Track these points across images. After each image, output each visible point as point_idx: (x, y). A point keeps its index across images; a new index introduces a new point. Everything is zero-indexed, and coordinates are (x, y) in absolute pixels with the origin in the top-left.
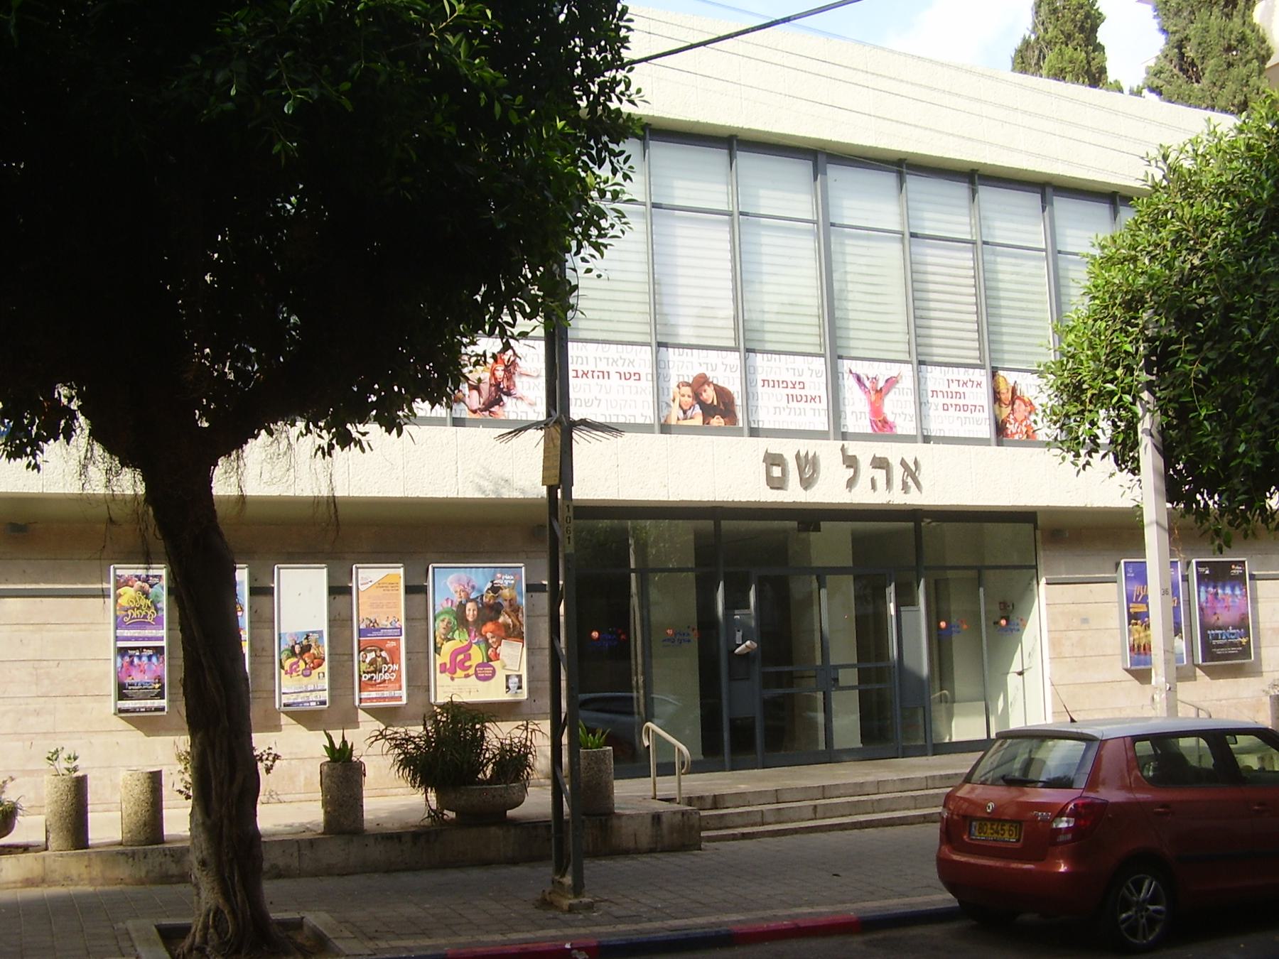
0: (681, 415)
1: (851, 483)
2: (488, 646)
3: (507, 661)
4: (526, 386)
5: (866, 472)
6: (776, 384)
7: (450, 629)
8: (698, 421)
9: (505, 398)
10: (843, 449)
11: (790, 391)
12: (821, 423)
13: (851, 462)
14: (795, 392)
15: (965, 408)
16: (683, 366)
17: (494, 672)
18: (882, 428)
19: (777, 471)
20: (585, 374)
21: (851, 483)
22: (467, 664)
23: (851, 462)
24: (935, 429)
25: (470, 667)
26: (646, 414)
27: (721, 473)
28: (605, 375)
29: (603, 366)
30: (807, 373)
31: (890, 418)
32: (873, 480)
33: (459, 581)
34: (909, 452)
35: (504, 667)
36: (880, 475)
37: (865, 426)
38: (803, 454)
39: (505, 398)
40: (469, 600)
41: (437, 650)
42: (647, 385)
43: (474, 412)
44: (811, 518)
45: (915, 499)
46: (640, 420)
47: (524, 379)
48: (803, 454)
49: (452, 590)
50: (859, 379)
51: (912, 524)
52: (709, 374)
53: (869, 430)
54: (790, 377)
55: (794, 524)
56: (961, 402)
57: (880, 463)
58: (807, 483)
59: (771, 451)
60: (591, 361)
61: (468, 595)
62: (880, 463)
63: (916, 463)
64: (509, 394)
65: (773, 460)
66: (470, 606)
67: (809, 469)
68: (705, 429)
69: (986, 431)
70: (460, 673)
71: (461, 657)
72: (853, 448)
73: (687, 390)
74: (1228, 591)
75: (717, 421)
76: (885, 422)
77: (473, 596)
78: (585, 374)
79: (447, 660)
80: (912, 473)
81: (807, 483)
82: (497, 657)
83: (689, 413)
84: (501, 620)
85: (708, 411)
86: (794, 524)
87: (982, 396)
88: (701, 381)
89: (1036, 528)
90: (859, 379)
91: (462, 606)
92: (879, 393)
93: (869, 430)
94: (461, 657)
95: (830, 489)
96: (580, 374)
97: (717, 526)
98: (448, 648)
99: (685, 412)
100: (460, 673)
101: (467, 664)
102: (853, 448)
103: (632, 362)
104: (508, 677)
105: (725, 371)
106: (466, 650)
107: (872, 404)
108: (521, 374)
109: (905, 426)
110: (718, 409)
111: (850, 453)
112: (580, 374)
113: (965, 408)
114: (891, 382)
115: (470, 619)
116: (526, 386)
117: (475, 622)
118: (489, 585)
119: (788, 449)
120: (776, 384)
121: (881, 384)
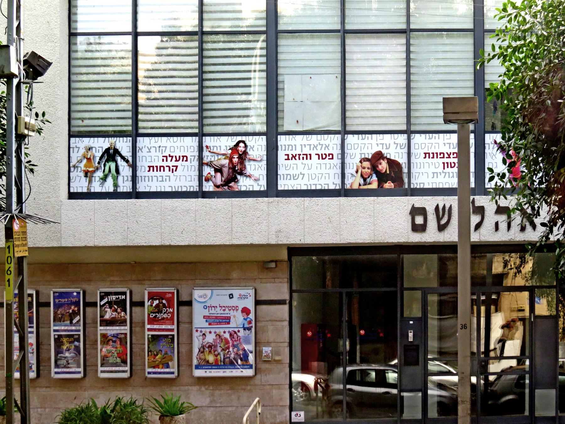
0: (362, 181)
4: (253, 167)
8: (375, 186)
9: (239, 177)
16: (361, 148)
28: (308, 156)
38: (441, 207)
39: (239, 177)
42: (337, 161)
47: (252, 163)
48: (441, 207)
52: (384, 151)
58: (441, 228)
59: (417, 205)
60: (299, 148)
64: (241, 174)
73: (367, 164)
75: (389, 185)
78: (294, 157)
83: (368, 180)
85: (382, 178)
88: (379, 156)
96: (290, 157)
99: (365, 180)
105: (393, 147)
108: (250, 160)
111: (477, 204)
112: (290, 157)
116: (253, 167)
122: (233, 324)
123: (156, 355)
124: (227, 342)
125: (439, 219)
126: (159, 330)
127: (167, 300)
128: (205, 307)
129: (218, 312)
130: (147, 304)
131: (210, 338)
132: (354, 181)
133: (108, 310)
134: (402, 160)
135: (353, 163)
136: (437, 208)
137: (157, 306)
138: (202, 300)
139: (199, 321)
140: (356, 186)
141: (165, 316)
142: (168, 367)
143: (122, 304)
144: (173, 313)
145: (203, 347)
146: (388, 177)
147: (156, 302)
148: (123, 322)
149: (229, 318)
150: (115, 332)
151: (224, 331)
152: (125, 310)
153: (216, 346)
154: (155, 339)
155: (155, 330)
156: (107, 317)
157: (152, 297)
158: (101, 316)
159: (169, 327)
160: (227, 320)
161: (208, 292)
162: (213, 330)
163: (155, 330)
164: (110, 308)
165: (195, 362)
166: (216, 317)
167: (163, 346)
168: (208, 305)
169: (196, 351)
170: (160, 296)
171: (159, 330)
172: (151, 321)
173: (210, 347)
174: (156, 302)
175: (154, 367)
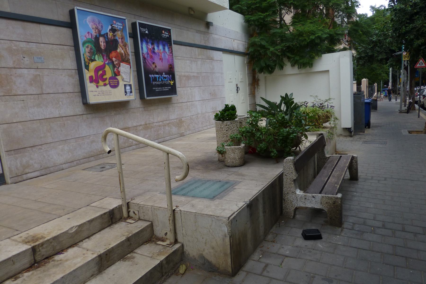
2: (114, 66)
3: (124, 77)
7: (92, 53)
17: (118, 82)
22: (105, 77)
25: (106, 79)
33: (93, 21)
35: (123, 80)
40: (101, 35)
41: (87, 67)
49: (90, 26)
61: (99, 32)
66: (101, 39)
70: (101, 83)
71: (100, 72)
77: (102, 33)
79: (92, 74)
82: (119, 72)
84: (118, 51)
91: (97, 39)
94: (100, 72)
98: (93, 65)
100: (101, 83)
101: (105, 77)
104: (125, 85)
106: (102, 68)
115: (103, 48)
117: (106, 49)
118: (110, 27)
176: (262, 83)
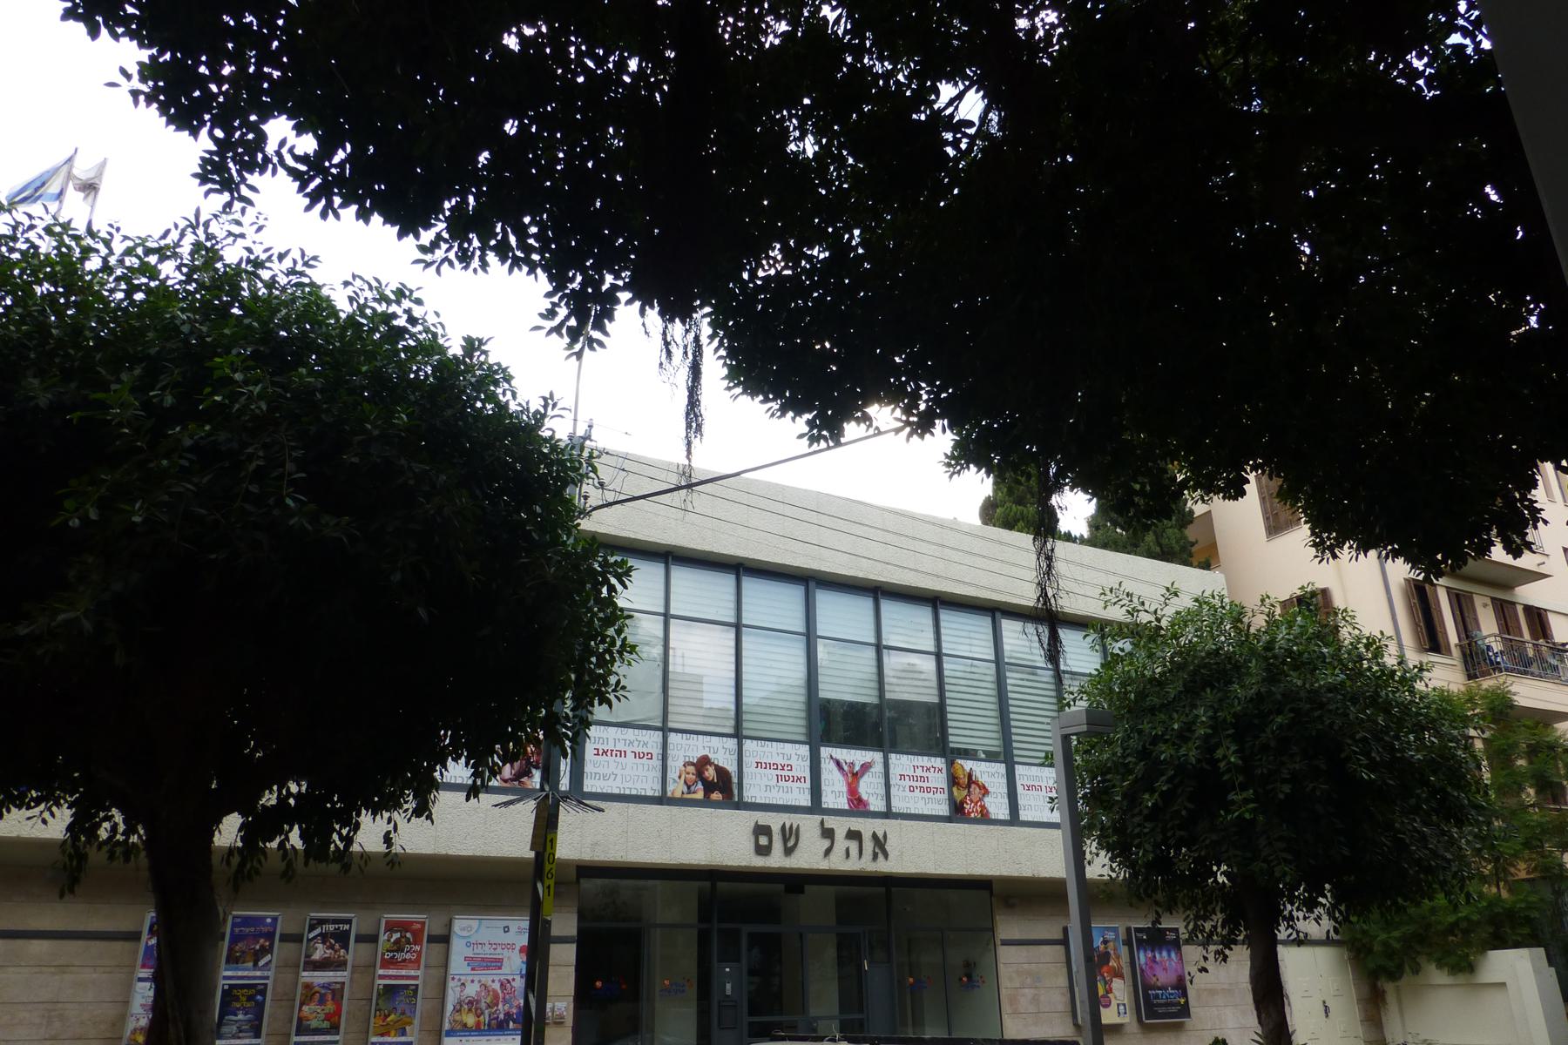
1: (828, 852)
5: (841, 842)
6: (767, 766)
8: (700, 795)
10: (822, 823)
11: (779, 772)
12: (805, 800)
13: (828, 834)
14: (783, 772)
15: (928, 790)
16: (685, 750)
18: (858, 806)
19: (763, 841)
20: (605, 752)
21: (828, 852)
23: (828, 834)
24: (898, 805)
26: (651, 787)
27: (719, 840)
29: (620, 746)
30: (794, 758)
31: (865, 797)
32: (847, 851)
34: (879, 826)
36: (854, 846)
37: (843, 803)
43: (506, 781)
44: (797, 882)
45: (883, 867)
46: (650, 793)
50: (838, 763)
51: (883, 890)
52: (711, 756)
53: (846, 807)
54: (779, 760)
55: (781, 887)
56: (925, 785)
57: (854, 835)
58: (788, 851)
62: (854, 835)
63: (885, 836)
65: (761, 830)
67: (791, 838)
68: (706, 803)
69: (943, 809)
72: (831, 822)
73: (691, 769)
74: (1165, 954)
75: (716, 796)
76: (860, 800)
78: (605, 752)
80: (880, 844)
81: (788, 851)
85: (709, 787)
86: (781, 887)
87: (939, 780)
88: (704, 762)
89: (991, 894)
90: (838, 763)
92: (854, 776)
93: (846, 807)
95: (810, 857)
97: (713, 886)
102: (831, 822)
103: (645, 744)
105: (722, 753)
107: (849, 785)
109: (877, 804)
110: (719, 787)
113: (928, 790)
114: (866, 767)
119: (775, 821)
120: (767, 766)
121: (857, 768)
122: (506, 969)
123: (386, 1016)
124: (496, 996)
125: (785, 840)
126: (396, 977)
127: (414, 933)
128: (468, 945)
129: (487, 952)
130: (383, 937)
131: (472, 990)
132: (676, 788)
133: (320, 946)
134: (732, 768)
135: (676, 765)
136: (784, 826)
137: (397, 941)
138: (465, 933)
139: (457, 965)
140: (678, 795)
141: (408, 956)
142: (404, 1034)
143: (342, 938)
144: (419, 954)
145: (460, 1003)
146: (719, 787)
147: (396, 936)
148: (340, 965)
149: (500, 961)
150: (326, 980)
151: (493, 980)
152: (346, 946)
153: (478, 1002)
154: (391, 991)
155: (390, 977)
156: (317, 956)
157: (391, 927)
158: (308, 956)
159: (412, 973)
160: (497, 963)
161: (475, 924)
162: (476, 978)
163: (390, 977)
164: (324, 943)
165: (447, 1026)
166: (483, 960)
167: (401, 1002)
168: (472, 940)
169: (449, 1008)
170: (403, 927)
171: (396, 977)
172: (386, 964)
173: (471, 1003)
174: (396, 936)
175: (382, 1035)
176: (1391, 998)
